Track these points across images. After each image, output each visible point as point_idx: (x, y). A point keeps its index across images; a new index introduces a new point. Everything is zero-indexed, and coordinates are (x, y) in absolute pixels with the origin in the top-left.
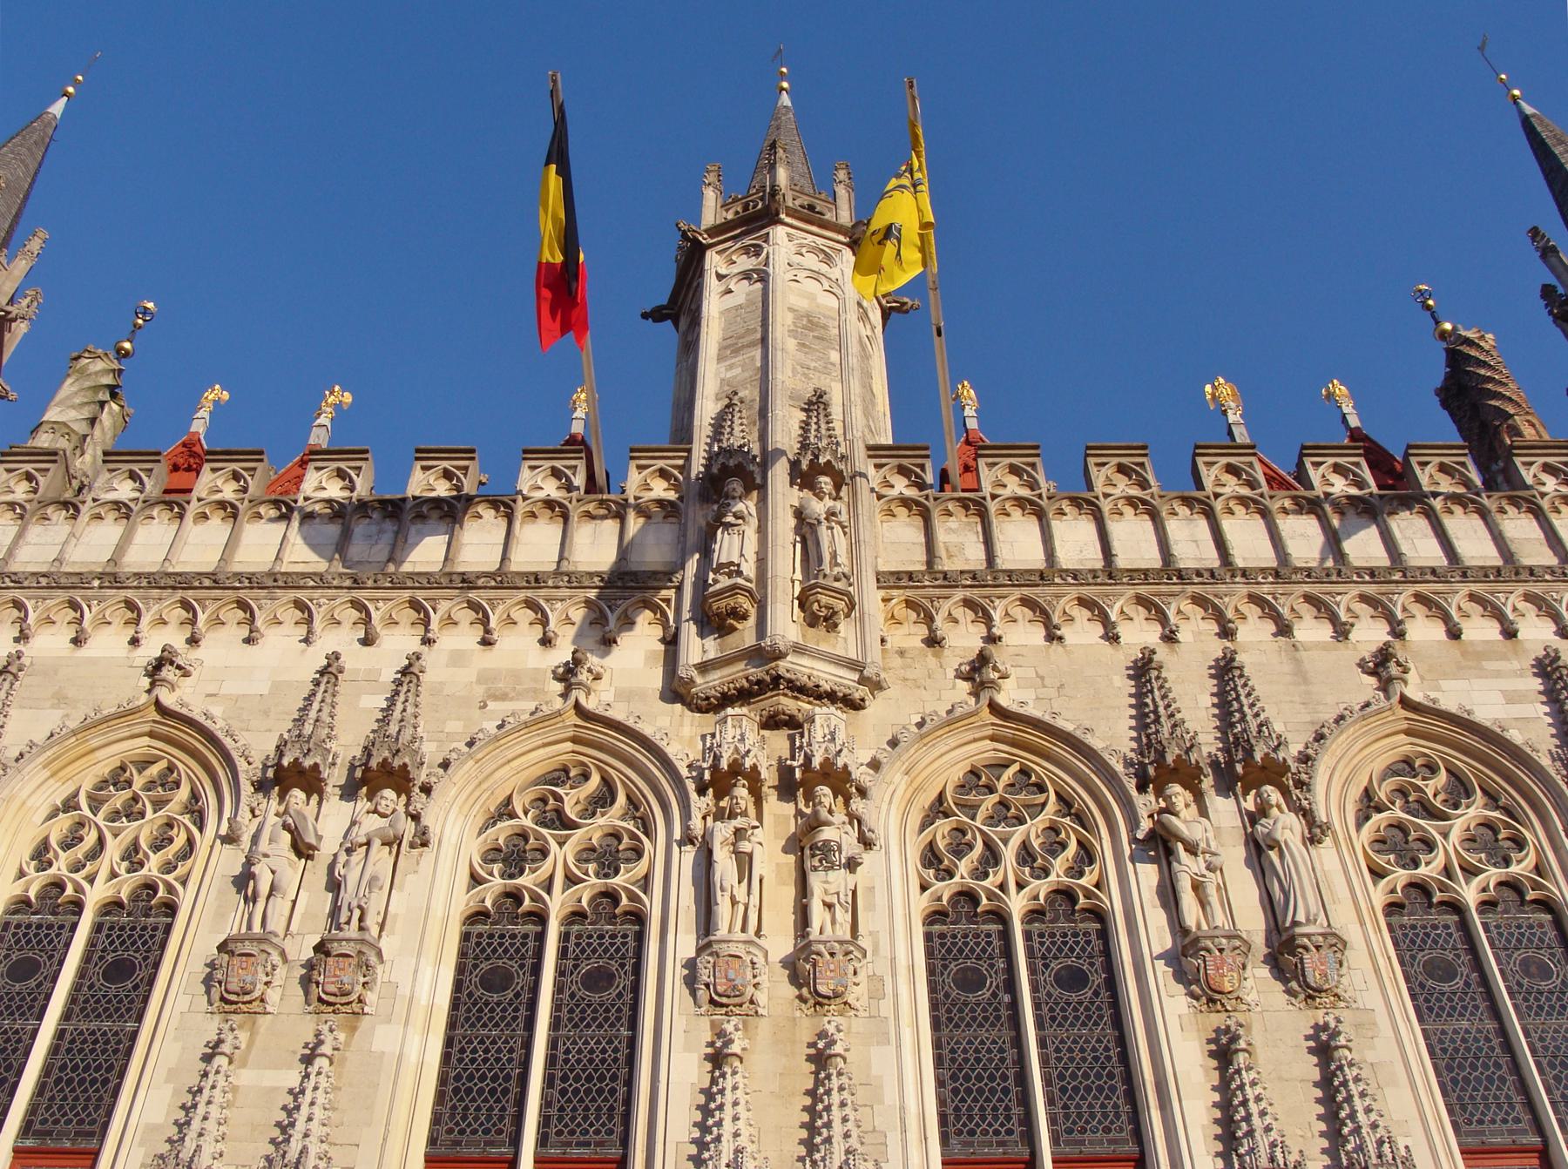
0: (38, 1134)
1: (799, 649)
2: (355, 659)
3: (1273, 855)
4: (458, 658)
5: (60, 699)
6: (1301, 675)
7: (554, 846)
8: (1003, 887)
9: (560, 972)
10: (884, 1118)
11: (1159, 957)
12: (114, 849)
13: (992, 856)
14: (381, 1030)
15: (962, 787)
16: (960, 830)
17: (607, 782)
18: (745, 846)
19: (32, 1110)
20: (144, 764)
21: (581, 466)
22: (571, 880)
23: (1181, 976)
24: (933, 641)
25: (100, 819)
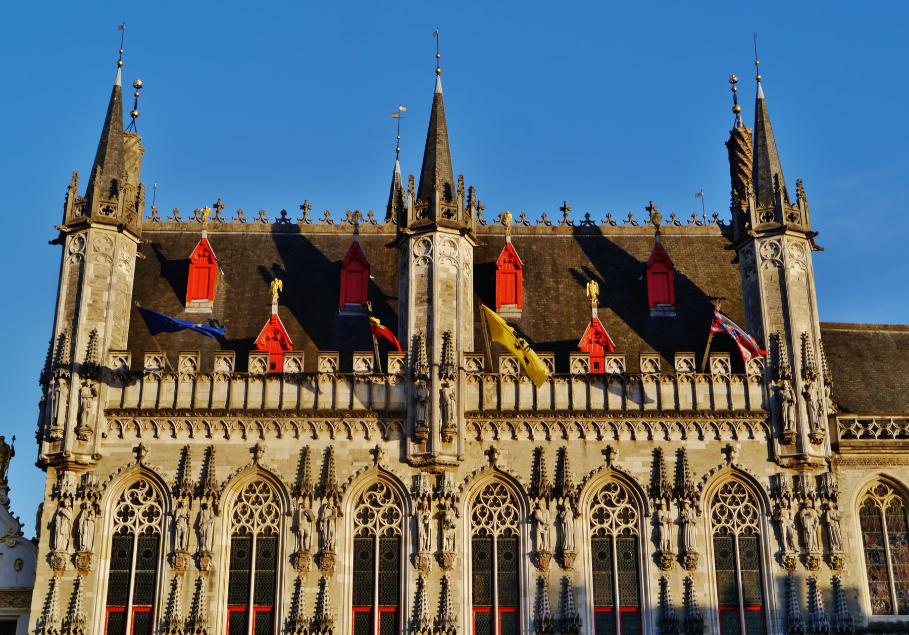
0: (258, 603)
1: (441, 454)
2: (314, 446)
3: (563, 525)
4: (343, 445)
5: (228, 462)
6: (585, 454)
7: (376, 513)
8: (493, 528)
9: (380, 553)
10: (460, 600)
11: (528, 554)
12: (256, 515)
13: (491, 517)
14: (338, 575)
15: (485, 493)
16: (483, 508)
17: (388, 489)
18: (427, 522)
19: (255, 596)
20: (258, 484)
21: (372, 357)
22: (381, 525)
23: (533, 561)
24: (479, 439)
25: (249, 504)
